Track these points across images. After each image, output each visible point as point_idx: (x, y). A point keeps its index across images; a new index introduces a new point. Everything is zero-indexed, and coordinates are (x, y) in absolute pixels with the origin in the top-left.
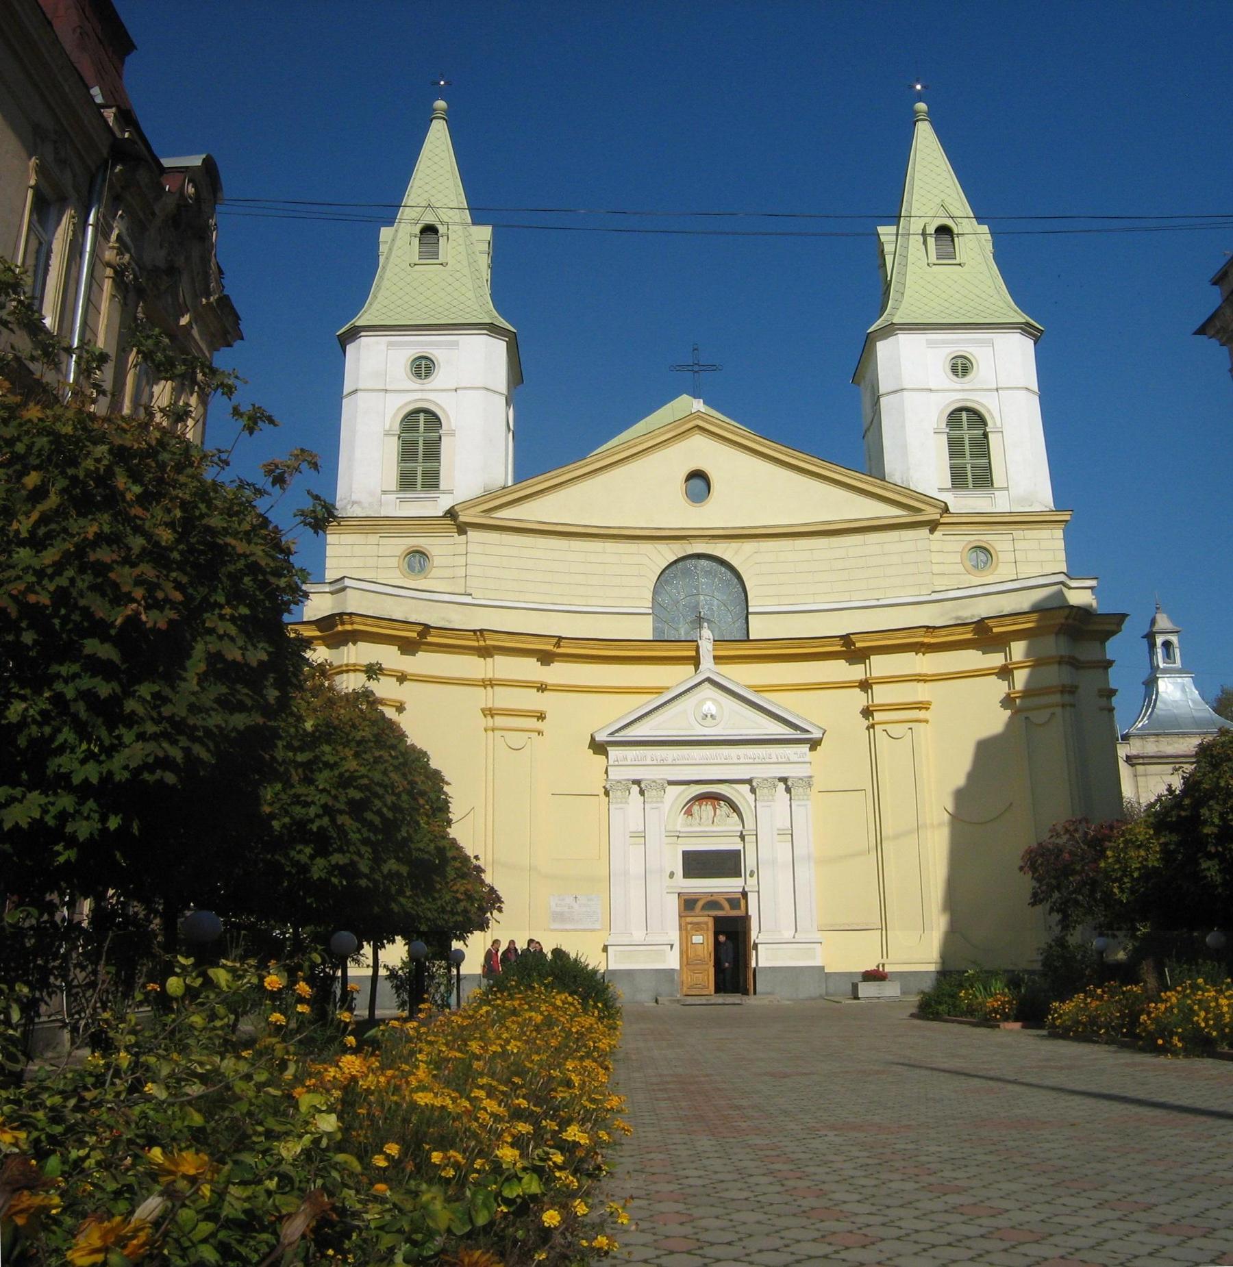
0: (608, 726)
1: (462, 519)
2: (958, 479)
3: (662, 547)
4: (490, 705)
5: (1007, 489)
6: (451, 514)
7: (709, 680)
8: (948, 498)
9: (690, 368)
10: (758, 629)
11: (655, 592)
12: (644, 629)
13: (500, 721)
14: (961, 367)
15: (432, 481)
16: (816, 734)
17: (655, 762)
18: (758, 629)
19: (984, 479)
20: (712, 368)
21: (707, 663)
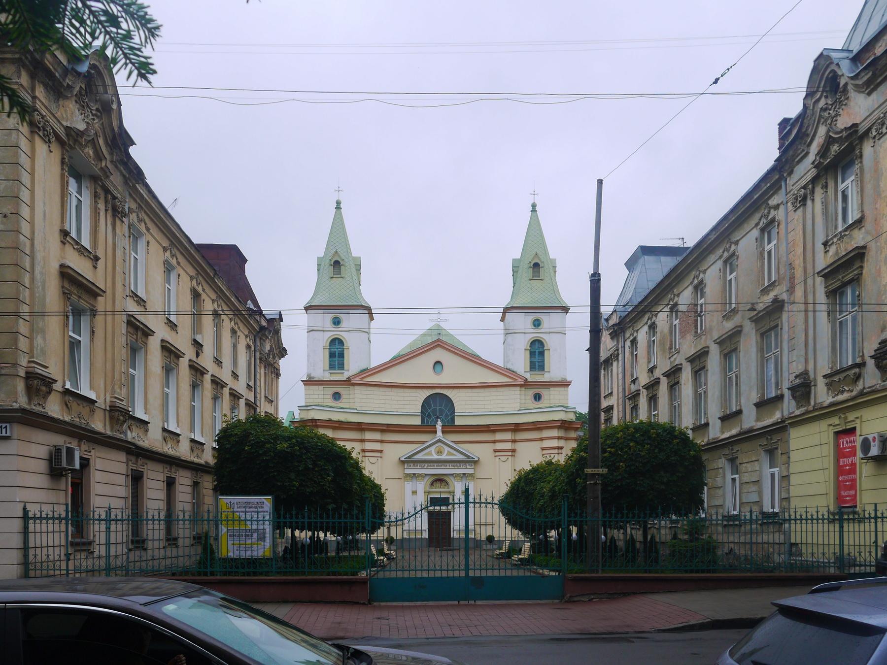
0: (404, 456)
1: (352, 382)
2: (533, 367)
4: (363, 448)
5: (549, 372)
6: (349, 379)
7: (439, 441)
8: (528, 376)
10: (458, 421)
11: (423, 406)
12: (417, 421)
13: (367, 454)
14: (537, 323)
15: (341, 366)
16: (476, 459)
18: (458, 421)
19: (542, 368)
21: (439, 433)
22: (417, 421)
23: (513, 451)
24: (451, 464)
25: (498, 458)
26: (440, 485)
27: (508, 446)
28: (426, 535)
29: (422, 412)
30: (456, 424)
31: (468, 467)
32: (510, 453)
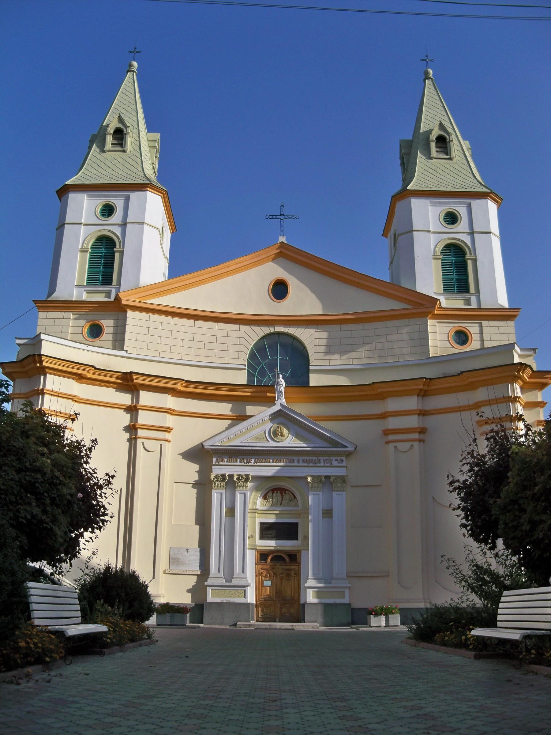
3: (256, 328)
9: (278, 217)
11: (252, 356)
12: (242, 378)
15: (107, 280)
16: (351, 448)
17: (243, 464)
18: (315, 380)
20: (293, 217)
21: (281, 401)
22: (242, 378)
23: (422, 431)
24: (301, 458)
25: (392, 445)
26: (280, 498)
27: (413, 422)
28: (251, 598)
29: (250, 365)
30: (310, 385)
31: (335, 463)
32: (416, 436)
